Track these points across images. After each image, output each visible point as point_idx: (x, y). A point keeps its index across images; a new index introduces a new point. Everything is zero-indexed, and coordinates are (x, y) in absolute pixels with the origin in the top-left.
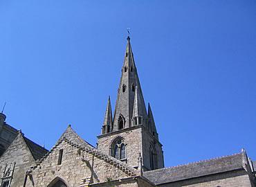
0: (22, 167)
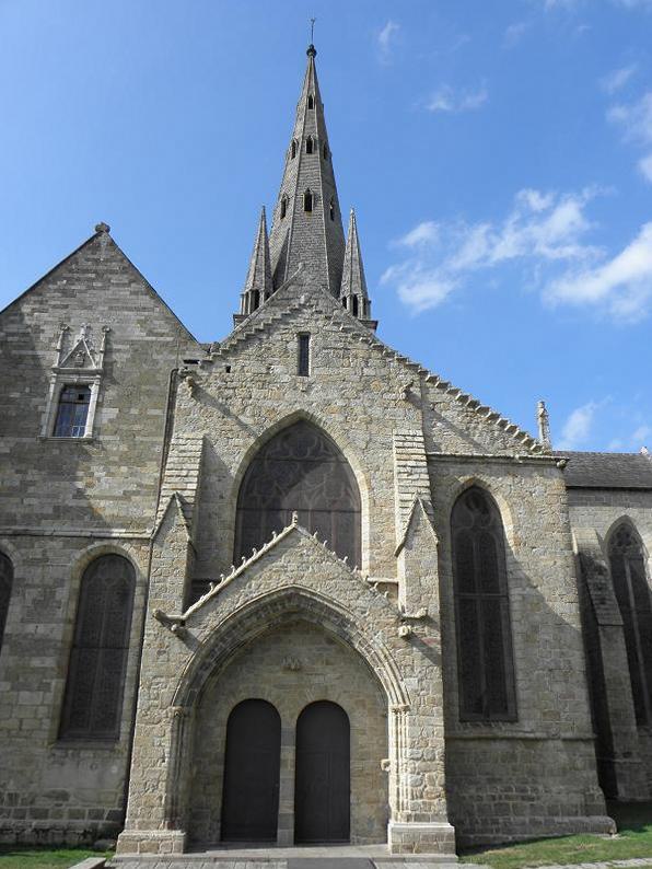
0: (140, 351)
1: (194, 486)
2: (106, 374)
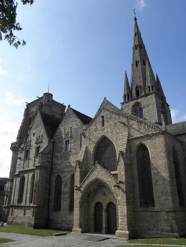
1: (82, 158)
2: (71, 137)
